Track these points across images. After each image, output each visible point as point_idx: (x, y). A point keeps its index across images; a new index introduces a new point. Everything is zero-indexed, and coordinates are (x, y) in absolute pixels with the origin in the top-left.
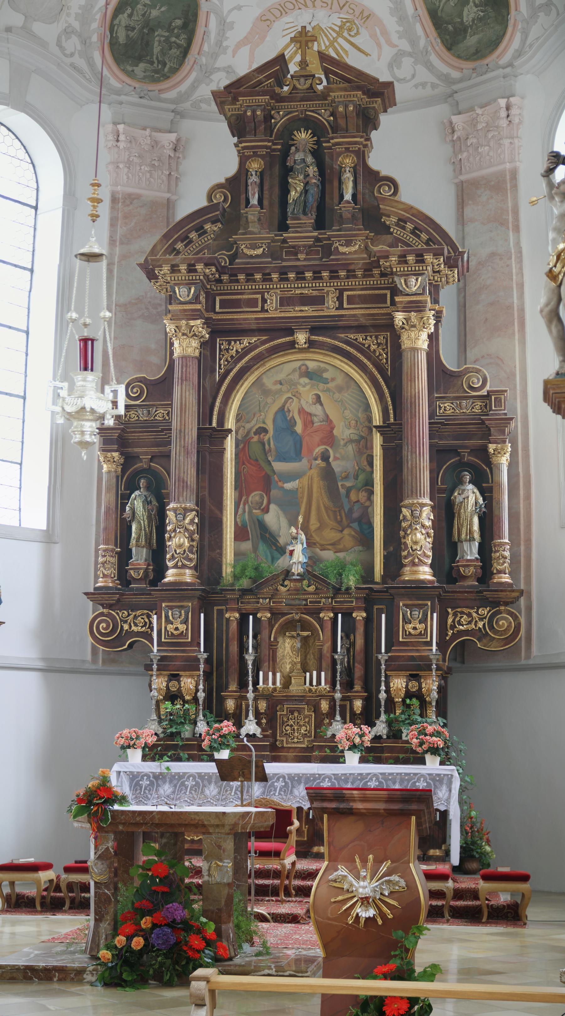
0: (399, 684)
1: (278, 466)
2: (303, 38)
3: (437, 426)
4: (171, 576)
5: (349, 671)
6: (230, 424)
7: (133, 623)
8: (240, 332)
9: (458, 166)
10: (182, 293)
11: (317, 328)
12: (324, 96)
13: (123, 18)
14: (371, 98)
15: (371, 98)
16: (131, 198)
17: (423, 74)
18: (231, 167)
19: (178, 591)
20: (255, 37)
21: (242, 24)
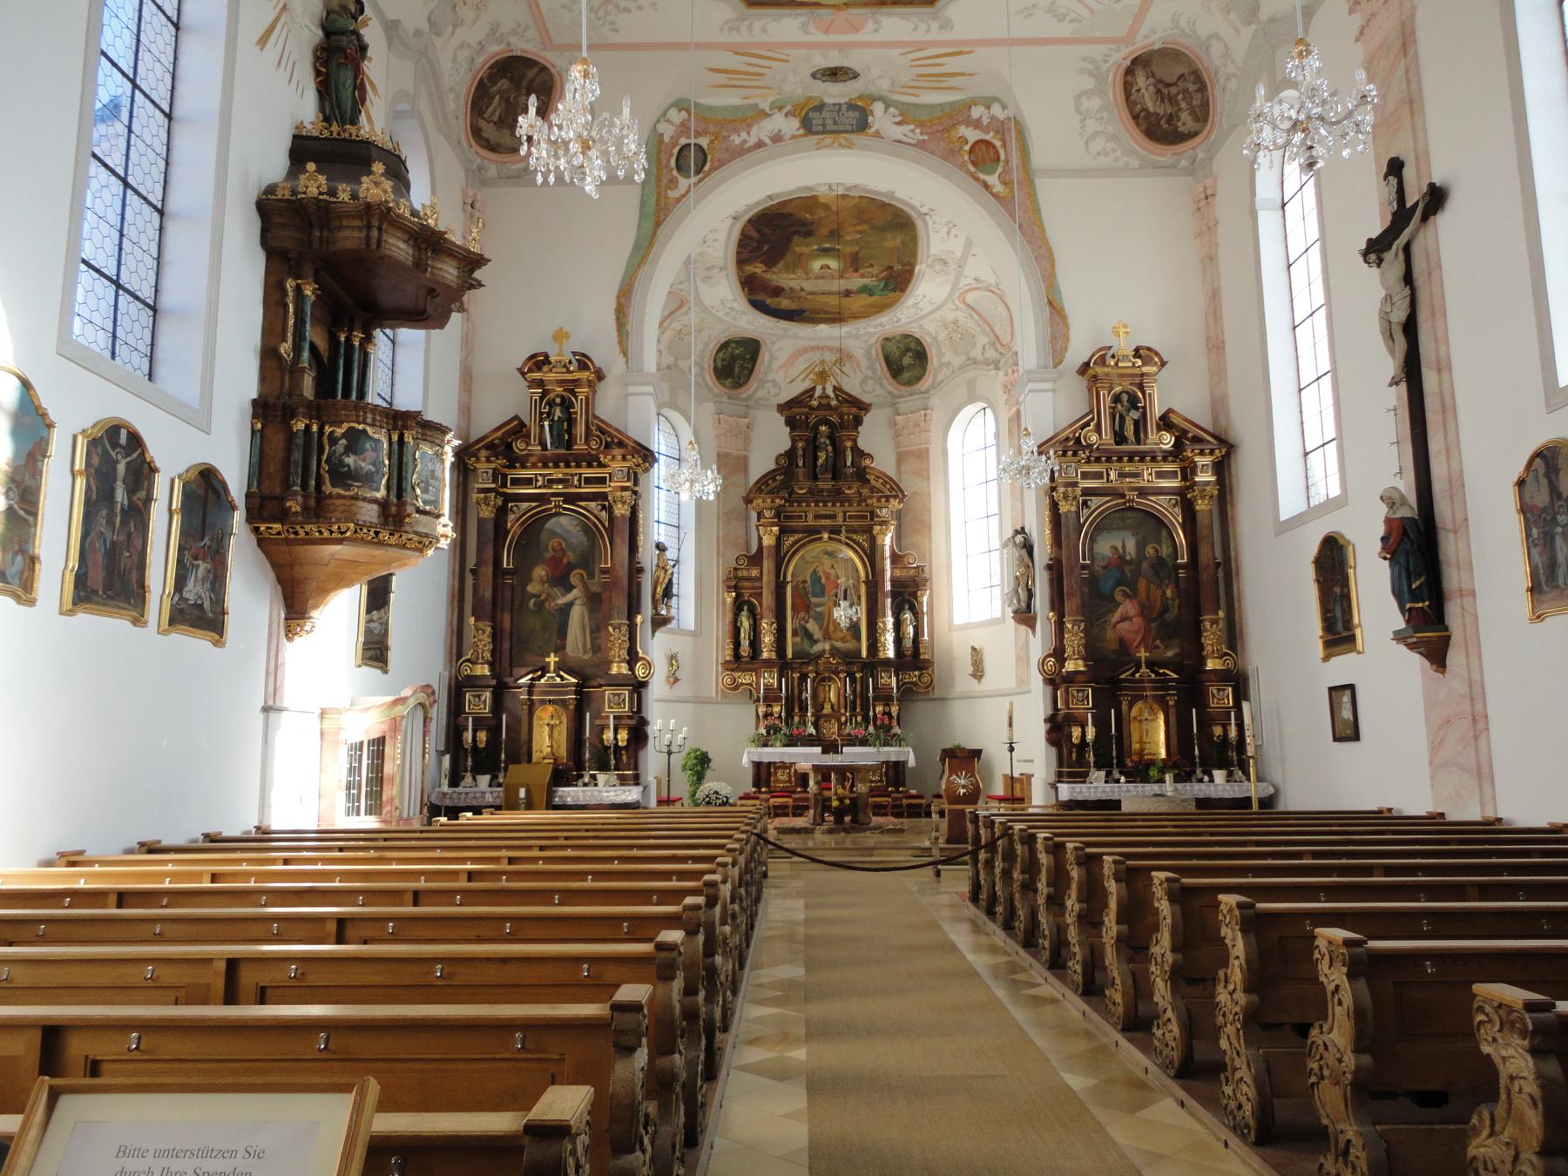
0: (879, 709)
1: (813, 600)
2: (823, 376)
3: (894, 582)
4: (765, 655)
5: (854, 703)
6: (789, 578)
7: (746, 678)
8: (793, 531)
9: (898, 445)
10: (768, 514)
11: (835, 531)
12: (836, 409)
13: (721, 355)
14: (855, 409)
15: (855, 409)
16: (727, 455)
17: (879, 390)
18: (786, 444)
19: (768, 664)
20: (788, 364)
21: (782, 357)
